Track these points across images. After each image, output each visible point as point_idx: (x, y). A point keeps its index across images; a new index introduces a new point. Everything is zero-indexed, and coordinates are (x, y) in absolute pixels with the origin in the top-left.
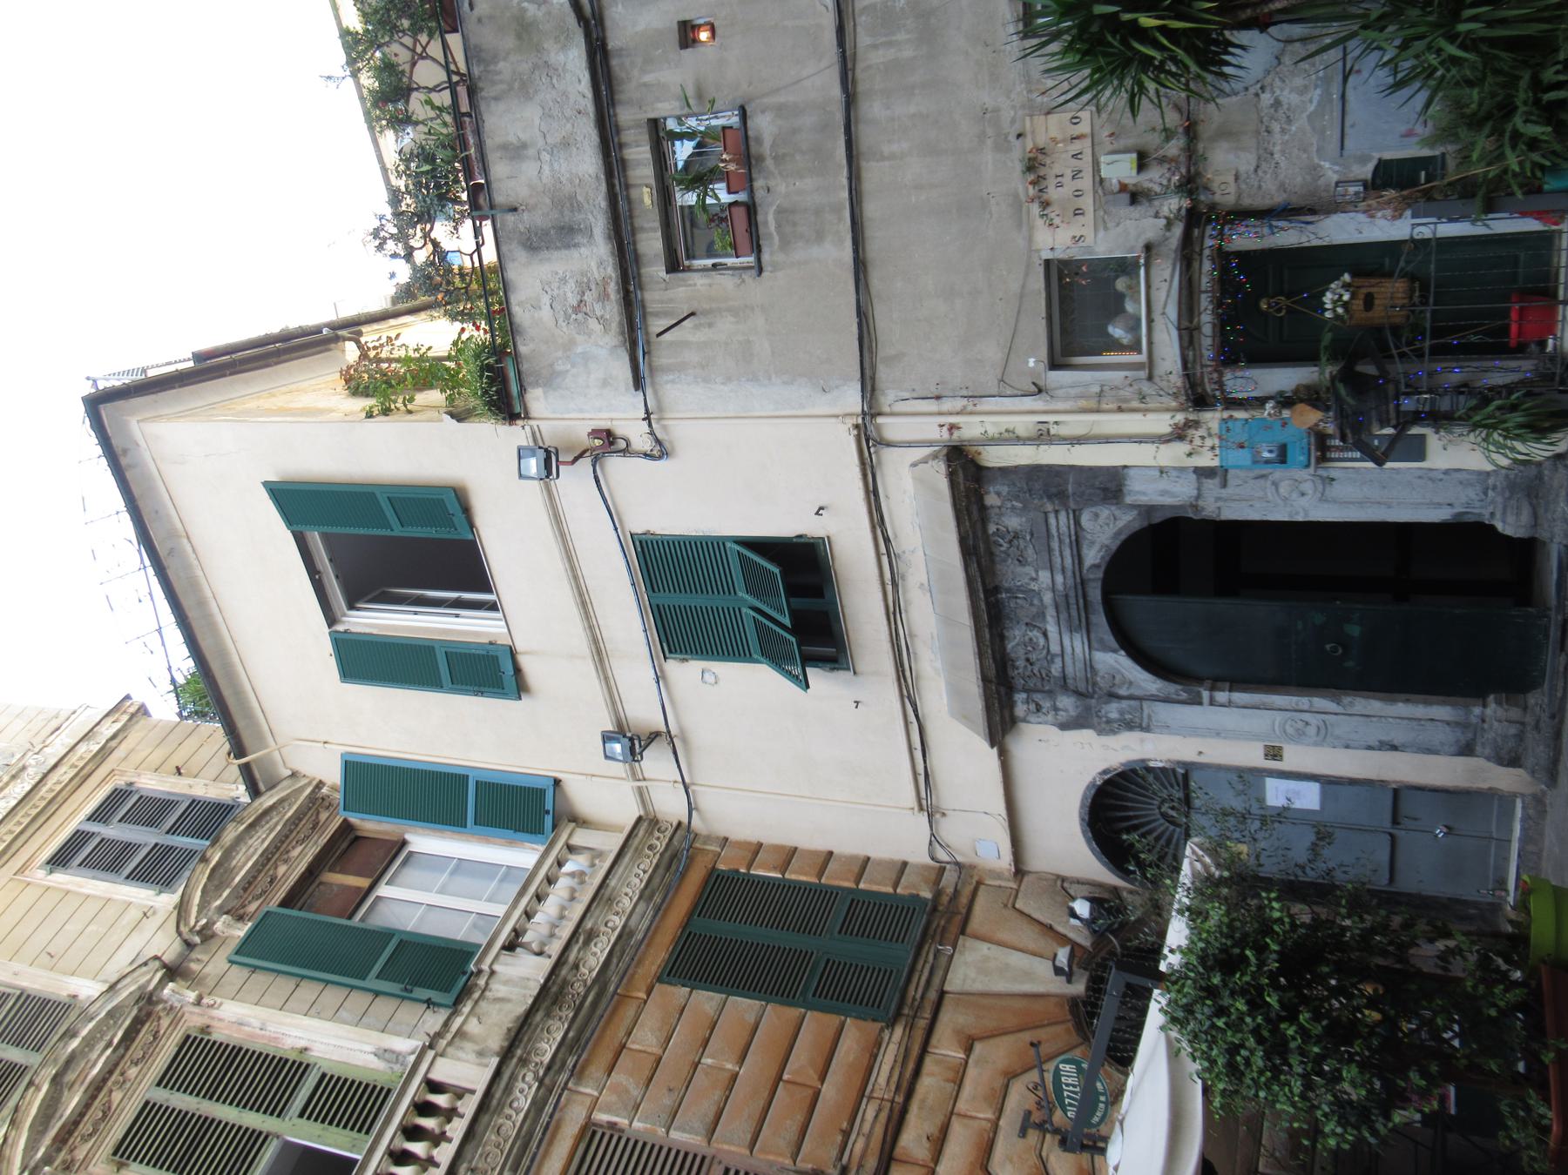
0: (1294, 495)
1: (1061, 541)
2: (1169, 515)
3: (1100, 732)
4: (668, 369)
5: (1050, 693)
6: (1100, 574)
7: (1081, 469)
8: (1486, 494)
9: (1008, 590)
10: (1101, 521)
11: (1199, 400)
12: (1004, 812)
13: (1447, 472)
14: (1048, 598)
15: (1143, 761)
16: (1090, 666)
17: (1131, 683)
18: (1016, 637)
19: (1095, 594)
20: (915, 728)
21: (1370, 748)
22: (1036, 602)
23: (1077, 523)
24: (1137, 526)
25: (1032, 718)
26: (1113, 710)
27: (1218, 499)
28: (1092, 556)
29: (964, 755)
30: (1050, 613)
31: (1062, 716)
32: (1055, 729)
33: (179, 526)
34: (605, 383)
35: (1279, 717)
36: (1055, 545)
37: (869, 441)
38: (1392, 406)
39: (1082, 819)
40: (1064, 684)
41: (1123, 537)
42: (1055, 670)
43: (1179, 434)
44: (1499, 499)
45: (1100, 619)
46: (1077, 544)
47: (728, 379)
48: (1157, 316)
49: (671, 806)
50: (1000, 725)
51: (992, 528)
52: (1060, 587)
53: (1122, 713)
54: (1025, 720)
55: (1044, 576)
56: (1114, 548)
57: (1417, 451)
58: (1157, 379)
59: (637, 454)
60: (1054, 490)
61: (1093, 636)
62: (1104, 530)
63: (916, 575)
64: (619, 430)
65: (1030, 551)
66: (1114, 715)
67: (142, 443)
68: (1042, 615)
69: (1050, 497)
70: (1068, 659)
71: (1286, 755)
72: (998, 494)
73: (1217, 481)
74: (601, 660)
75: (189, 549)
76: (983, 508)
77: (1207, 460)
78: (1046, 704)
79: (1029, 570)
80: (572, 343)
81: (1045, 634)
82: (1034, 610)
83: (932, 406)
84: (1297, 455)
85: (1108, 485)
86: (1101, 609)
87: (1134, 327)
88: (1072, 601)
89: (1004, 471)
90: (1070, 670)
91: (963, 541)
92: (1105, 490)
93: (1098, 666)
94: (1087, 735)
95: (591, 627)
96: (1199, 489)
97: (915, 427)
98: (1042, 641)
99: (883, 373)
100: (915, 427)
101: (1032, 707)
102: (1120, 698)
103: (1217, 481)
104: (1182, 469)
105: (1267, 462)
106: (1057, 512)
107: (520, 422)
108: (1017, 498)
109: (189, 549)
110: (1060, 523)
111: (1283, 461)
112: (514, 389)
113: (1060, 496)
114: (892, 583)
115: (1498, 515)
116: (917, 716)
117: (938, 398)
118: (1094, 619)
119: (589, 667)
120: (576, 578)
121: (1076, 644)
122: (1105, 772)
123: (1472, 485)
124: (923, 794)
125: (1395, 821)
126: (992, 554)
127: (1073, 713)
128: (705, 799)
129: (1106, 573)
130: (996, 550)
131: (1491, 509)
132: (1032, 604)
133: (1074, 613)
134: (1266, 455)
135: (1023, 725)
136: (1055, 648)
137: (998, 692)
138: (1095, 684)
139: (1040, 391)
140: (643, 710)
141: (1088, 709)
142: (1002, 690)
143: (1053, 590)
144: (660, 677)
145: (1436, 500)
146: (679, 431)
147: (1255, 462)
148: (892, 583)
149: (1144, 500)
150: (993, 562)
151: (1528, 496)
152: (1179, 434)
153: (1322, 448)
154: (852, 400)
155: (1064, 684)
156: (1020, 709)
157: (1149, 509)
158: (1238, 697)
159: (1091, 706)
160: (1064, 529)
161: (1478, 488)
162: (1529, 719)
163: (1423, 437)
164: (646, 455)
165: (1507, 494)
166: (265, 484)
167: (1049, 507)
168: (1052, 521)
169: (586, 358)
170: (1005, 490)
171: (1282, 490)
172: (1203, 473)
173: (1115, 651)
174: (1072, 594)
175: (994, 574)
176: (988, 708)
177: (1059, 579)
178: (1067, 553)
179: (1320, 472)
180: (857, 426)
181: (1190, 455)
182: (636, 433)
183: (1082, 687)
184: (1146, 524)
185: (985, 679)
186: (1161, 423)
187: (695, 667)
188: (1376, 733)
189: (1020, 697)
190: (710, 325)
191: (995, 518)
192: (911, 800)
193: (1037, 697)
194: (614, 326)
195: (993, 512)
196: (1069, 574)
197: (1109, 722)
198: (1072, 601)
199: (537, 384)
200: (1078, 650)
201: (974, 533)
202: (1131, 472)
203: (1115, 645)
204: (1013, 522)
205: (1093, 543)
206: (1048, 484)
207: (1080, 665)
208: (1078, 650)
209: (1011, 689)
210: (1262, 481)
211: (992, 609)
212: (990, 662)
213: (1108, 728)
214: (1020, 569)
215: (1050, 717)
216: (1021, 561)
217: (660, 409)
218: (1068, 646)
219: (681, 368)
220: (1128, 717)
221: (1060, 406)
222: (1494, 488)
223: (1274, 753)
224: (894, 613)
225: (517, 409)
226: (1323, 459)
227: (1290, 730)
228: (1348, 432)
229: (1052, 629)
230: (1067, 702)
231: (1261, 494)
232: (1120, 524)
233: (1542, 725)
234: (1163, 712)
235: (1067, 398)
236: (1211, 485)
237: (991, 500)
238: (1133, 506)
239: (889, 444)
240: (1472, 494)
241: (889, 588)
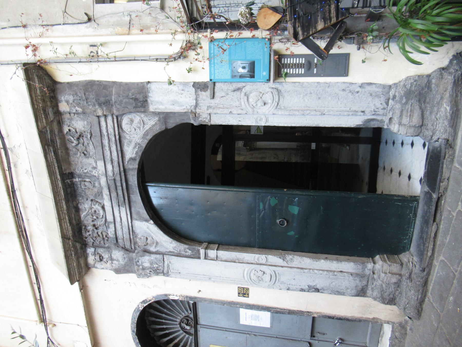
0: (260, 103)
2: (179, 121)
3: (139, 276)
6: (136, 165)
8: (387, 104)
9: (80, 176)
10: (135, 124)
13: (362, 86)
14: (103, 181)
15: (166, 295)
16: (132, 231)
17: (157, 243)
18: (85, 207)
19: (133, 180)
20: (32, 269)
21: (302, 290)
22: (97, 184)
23: (120, 126)
24: (158, 129)
25: (98, 265)
26: (146, 261)
27: (209, 107)
28: (131, 152)
30: (106, 191)
32: (112, 273)
35: (247, 268)
36: (106, 142)
38: (333, 6)
41: (149, 137)
43: (182, 55)
44: (398, 106)
46: (120, 142)
50: (78, 270)
51: (66, 129)
52: (110, 173)
53: (152, 264)
54: (94, 266)
56: (144, 146)
57: (341, 66)
58: (167, 10)
60: (102, 99)
61: (133, 209)
62: (137, 132)
65: (91, 147)
66: (147, 265)
68: (100, 194)
69: (100, 105)
70: (118, 225)
71: (251, 292)
72: (67, 102)
73: (208, 93)
76: (58, 113)
77: (203, 76)
78: (106, 256)
79: (91, 161)
81: (103, 208)
82: (96, 190)
83: (20, 32)
84: (262, 71)
85: (138, 97)
88: (119, 184)
89: (70, 85)
90: (119, 233)
91: (42, 134)
92: (136, 99)
93: (137, 231)
94: (132, 277)
96: (196, 100)
98: (101, 212)
101: (97, 257)
102: (150, 253)
103: (208, 93)
104: (185, 84)
105: (241, 77)
106: (106, 116)
108: (78, 105)
111: (252, 76)
113: (107, 103)
115: (396, 119)
116: (32, 261)
117: (24, 26)
122: (144, 302)
123: (378, 96)
125: (312, 336)
126: (67, 149)
127: (122, 262)
131: (390, 115)
132: (94, 186)
134: (241, 71)
135: (94, 270)
136: (110, 218)
137: (74, 246)
138: (135, 243)
139: (89, 20)
141: (131, 260)
142: (78, 245)
145: (354, 108)
147: (233, 76)
149: (162, 108)
150: (68, 154)
151: (419, 101)
152: (182, 55)
153: (279, 67)
156: (91, 259)
158: (223, 254)
159: (133, 256)
160: (111, 130)
161: (383, 99)
162: (405, 272)
163: (347, 56)
165: (404, 101)
170: (71, 98)
171: (251, 100)
172: (200, 87)
173: (146, 221)
174: (118, 178)
175: (69, 164)
177: (109, 167)
178: (114, 148)
179: (277, 85)
181: (190, 71)
183: (128, 245)
184: (163, 128)
185: (64, 237)
188: (306, 280)
189: (90, 250)
191: (67, 121)
192: (36, 318)
193: (100, 251)
195: (66, 116)
196: (116, 164)
197: (143, 269)
198: (119, 184)
200: (124, 219)
201: (52, 131)
202: (152, 87)
203: (147, 217)
204: (79, 125)
205: (130, 142)
206: (99, 95)
207: (126, 230)
208: (124, 219)
209: (85, 245)
210: (238, 93)
211: (67, 190)
213: (144, 273)
214: (85, 160)
215: (108, 265)
220: (155, 266)
221: (104, 31)
222: (394, 97)
223: (244, 292)
226: (278, 74)
227: (253, 277)
228: (299, 30)
230: (118, 254)
231: (237, 104)
232: (147, 127)
233: (413, 276)
234: (177, 263)
236: (205, 95)
237: (63, 107)
240: (378, 103)
241: (7, 173)
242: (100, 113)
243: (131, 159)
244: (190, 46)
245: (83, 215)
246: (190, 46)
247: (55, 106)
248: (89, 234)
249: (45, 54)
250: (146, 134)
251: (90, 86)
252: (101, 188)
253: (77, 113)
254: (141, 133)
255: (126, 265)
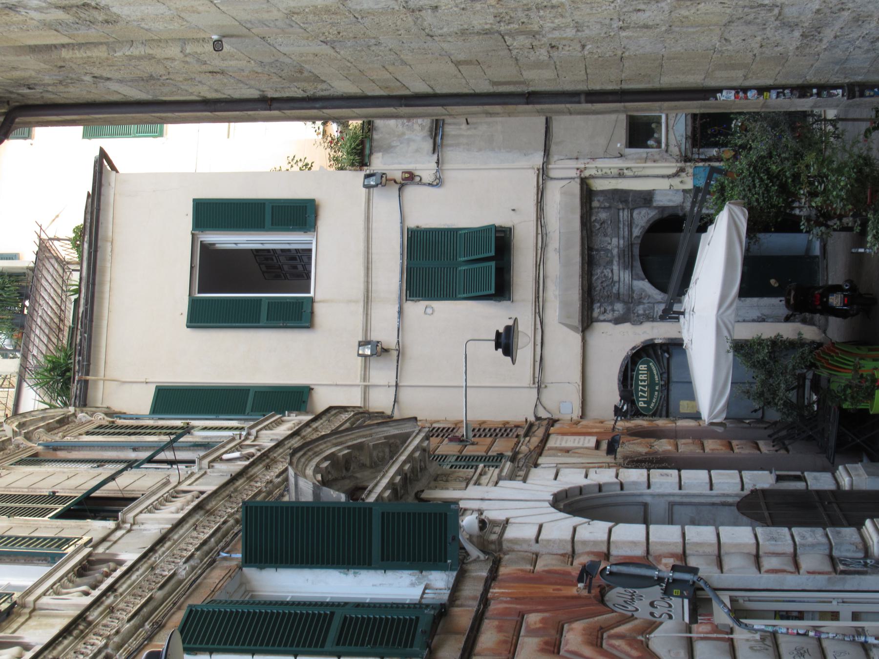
1: (624, 224)
3: (634, 323)
4: (451, 145)
5: (612, 304)
6: (639, 241)
7: (635, 191)
9: (597, 250)
11: (687, 159)
12: (580, 384)
14: (615, 252)
15: (652, 340)
16: (631, 288)
17: (649, 296)
18: (598, 271)
19: (636, 251)
21: (753, 321)
23: (632, 216)
24: (657, 217)
25: (602, 318)
28: (637, 232)
29: (564, 343)
30: (616, 259)
31: (616, 314)
32: (610, 326)
33: (110, 234)
34: (417, 151)
36: (621, 226)
37: (543, 174)
39: (619, 380)
40: (618, 297)
42: (615, 290)
43: (676, 175)
45: (638, 264)
46: (631, 225)
47: (480, 150)
48: (670, 129)
49: (381, 401)
50: (587, 322)
51: (593, 218)
52: (621, 246)
53: (645, 311)
54: (598, 321)
55: (615, 241)
59: (425, 184)
62: (643, 218)
63: (554, 243)
64: (417, 173)
65: (609, 229)
66: (641, 312)
67: (113, 184)
68: (610, 262)
69: (621, 202)
72: (599, 201)
74: (367, 302)
75: (109, 249)
76: (591, 208)
79: (608, 239)
80: (403, 134)
85: (646, 198)
86: (638, 258)
87: (659, 142)
88: (626, 253)
89: (602, 192)
90: (621, 290)
91: (582, 217)
92: (645, 199)
93: (634, 288)
94: (627, 326)
95: (368, 282)
97: (565, 169)
98: (610, 275)
99: (553, 148)
100: (565, 169)
101: (602, 309)
102: (644, 304)
104: (678, 190)
106: (623, 209)
107: (365, 168)
109: (109, 249)
110: (624, 215)
112: (367, 152)
113: (626, 202)
114: (542, 249)
118: (635, 264)
119: (360, 308)
120: (368, 253)
121: (626, 276)
122: (633, 349)
124: (537, 375)
126: (592, 232)
127: (622, 312)
128: (406, 395)
129: (642, 240)
130: (594, 230)
133: (626, 259)
135: (596, 324)
136: (616, 278)
138: (633, 298)
140: (385, 333)
143: (618, 247)
144: (401, 312)
146: (449, 175)
148: (542, 249)
149: (661, 204)
152: (676, 175)
154: (538, 159)
155: (618, 297)
156: (595, 314)
157: (663, 209)
160: (625, 217)
164: (430, 184)
166: (194, 200)
167: (621, 206)
168: (621, 214)
169: (409, 141)
170: (601, 199)
173: (643, 280)
174: (626, 249)
176: (583, 306)
177: (621, 242)
178: (626, 229)
180: (538, 170)
181: (681, 182)
182: (428, 175)
183: (626, 299)
186: (671, 167)
187: (423, 304)
188: (756, 314)
190: (475, 128)
194: (427, 128)
195: (594, 211)
197: (638, 316)
198: (626, 253)
199: (380, 151)
203: (644, 276)
204: (603, 215)
205: (637, 225)
206: (621, 197)
207: (626, 287)
208: (627, 279)
211: (590, 259)
212: (586, 282)
213: (638, 320)
216: (606, 235)
217: (443, 163)
218: (622, 277)
219: (458, 145)
224: (540, 263)
225: (367, 160)
229: (615, 268)
232: (650, 216)
235: (632, 159)
237: (595, 204)
238: (656, 208)
239: (552, 179)
241: (539, 251)
242: (621, 206)
243: (637, 237)
244: (682, 170)
245: (594, 278)
246: (682, 170)
247: (590, 204)
248: (596, 294)
249: (586, 174)
250: (648, 221)
251: (615, 192)
252: (613, 256)
253: (605, 208)
254: (645, 219)
255: (624, 314)
